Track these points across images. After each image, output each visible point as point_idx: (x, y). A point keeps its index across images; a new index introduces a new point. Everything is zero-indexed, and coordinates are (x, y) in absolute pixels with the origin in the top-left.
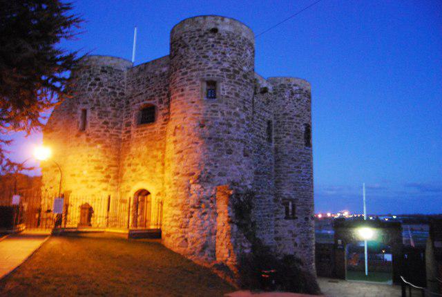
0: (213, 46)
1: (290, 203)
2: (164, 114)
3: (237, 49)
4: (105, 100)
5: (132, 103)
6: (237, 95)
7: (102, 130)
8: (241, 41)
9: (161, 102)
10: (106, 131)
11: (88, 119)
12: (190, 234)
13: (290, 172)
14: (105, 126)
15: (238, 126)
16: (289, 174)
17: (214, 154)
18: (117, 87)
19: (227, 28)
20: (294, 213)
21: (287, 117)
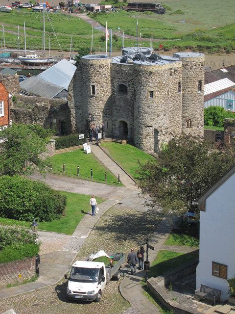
2: (131, 92)
6: (161, 94)
9: (129, 86)
10: (104, 95)
19: (156, 69)
20: (190, 125)
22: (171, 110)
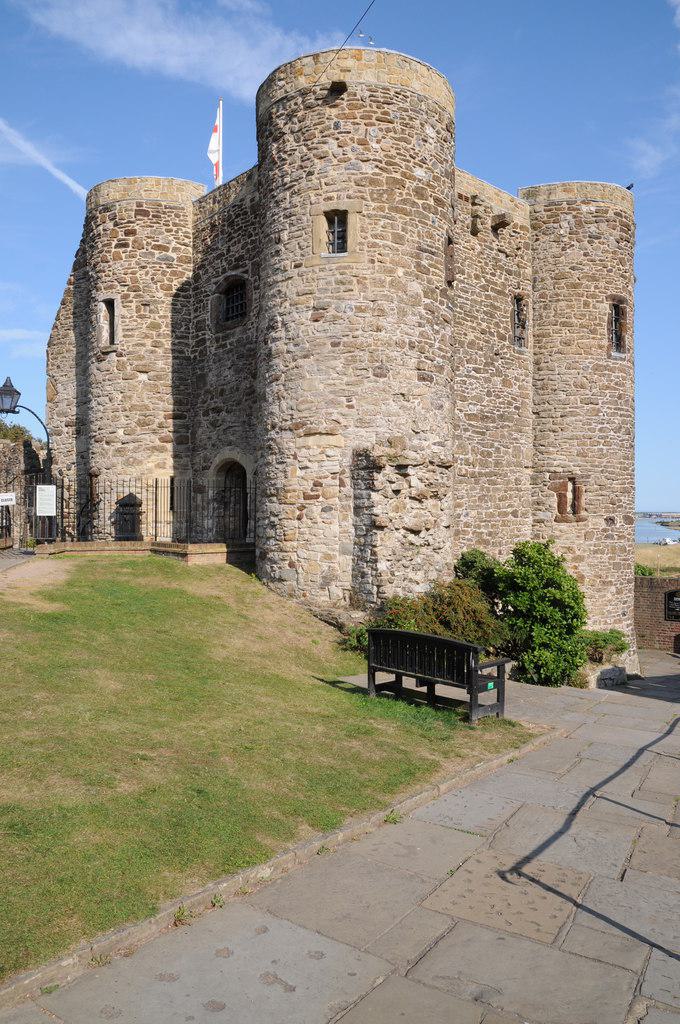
0: (337, 126)
1: (570, 486)
3: (399, 127)
4: (149, 277)
5: (204, 278)
7: (148, 342)
8: (406, 105)
11: (117, 320)
12: (303, 553)
13: (572, 414)
14: (154, 333)
15: (402, 313)
16: (568, 420)
17: (346, 379)
18: (173, 244)
19: (369, 77)
20: (575, 509)
21: (563, 283)
22: (474, 410)
